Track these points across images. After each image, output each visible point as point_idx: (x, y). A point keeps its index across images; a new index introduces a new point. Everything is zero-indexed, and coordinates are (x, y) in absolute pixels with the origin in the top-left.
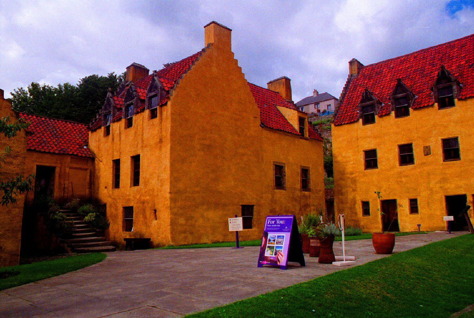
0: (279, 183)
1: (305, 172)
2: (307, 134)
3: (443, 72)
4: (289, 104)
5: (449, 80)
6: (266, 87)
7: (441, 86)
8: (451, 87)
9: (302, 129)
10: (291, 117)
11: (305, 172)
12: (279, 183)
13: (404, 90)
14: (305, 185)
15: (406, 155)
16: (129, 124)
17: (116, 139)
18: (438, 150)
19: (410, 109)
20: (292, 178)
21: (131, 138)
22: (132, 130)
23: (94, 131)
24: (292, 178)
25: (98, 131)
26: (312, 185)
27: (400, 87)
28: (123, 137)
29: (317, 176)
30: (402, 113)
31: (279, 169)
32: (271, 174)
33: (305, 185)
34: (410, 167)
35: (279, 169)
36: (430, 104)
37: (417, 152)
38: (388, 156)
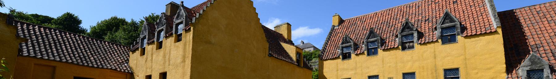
3: (407, 23)
4: (290, 42)
6: (273, 29)
7: (404, 33)
8: (412, 34)
9: (298, 61)
10: (291, 51)
17: (149, 58)
19: (379, 50)
21: (161, 58)
22: (161, 51)
23: (134, 51)
25: (137, 52)
27: (372, 33)
28: (154, 56)
30: (372, 52)
36: (396, 46)
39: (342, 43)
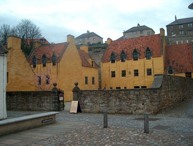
0: (86, 82)
1: (93, 78)
2: (94, 66)
5: (137, 52)
9: (92, 66)
11: (93, 78)
12: (86, 82)
13: (124, 54)
14: (93, 83)
15: (124, 74)
16: (44, 66)
18: (133, 73)
20: (90, 81)
22: (45, 68)
24: (90, 81)
26: (95, 82)
29: (97, 81)
31: (86, 78)
32: (84, 80)
33: (93, 83)
34: (125, 77)
35: (86, 78)
37: (127, 73)
38: (118, 74)
39: (111, 55)
